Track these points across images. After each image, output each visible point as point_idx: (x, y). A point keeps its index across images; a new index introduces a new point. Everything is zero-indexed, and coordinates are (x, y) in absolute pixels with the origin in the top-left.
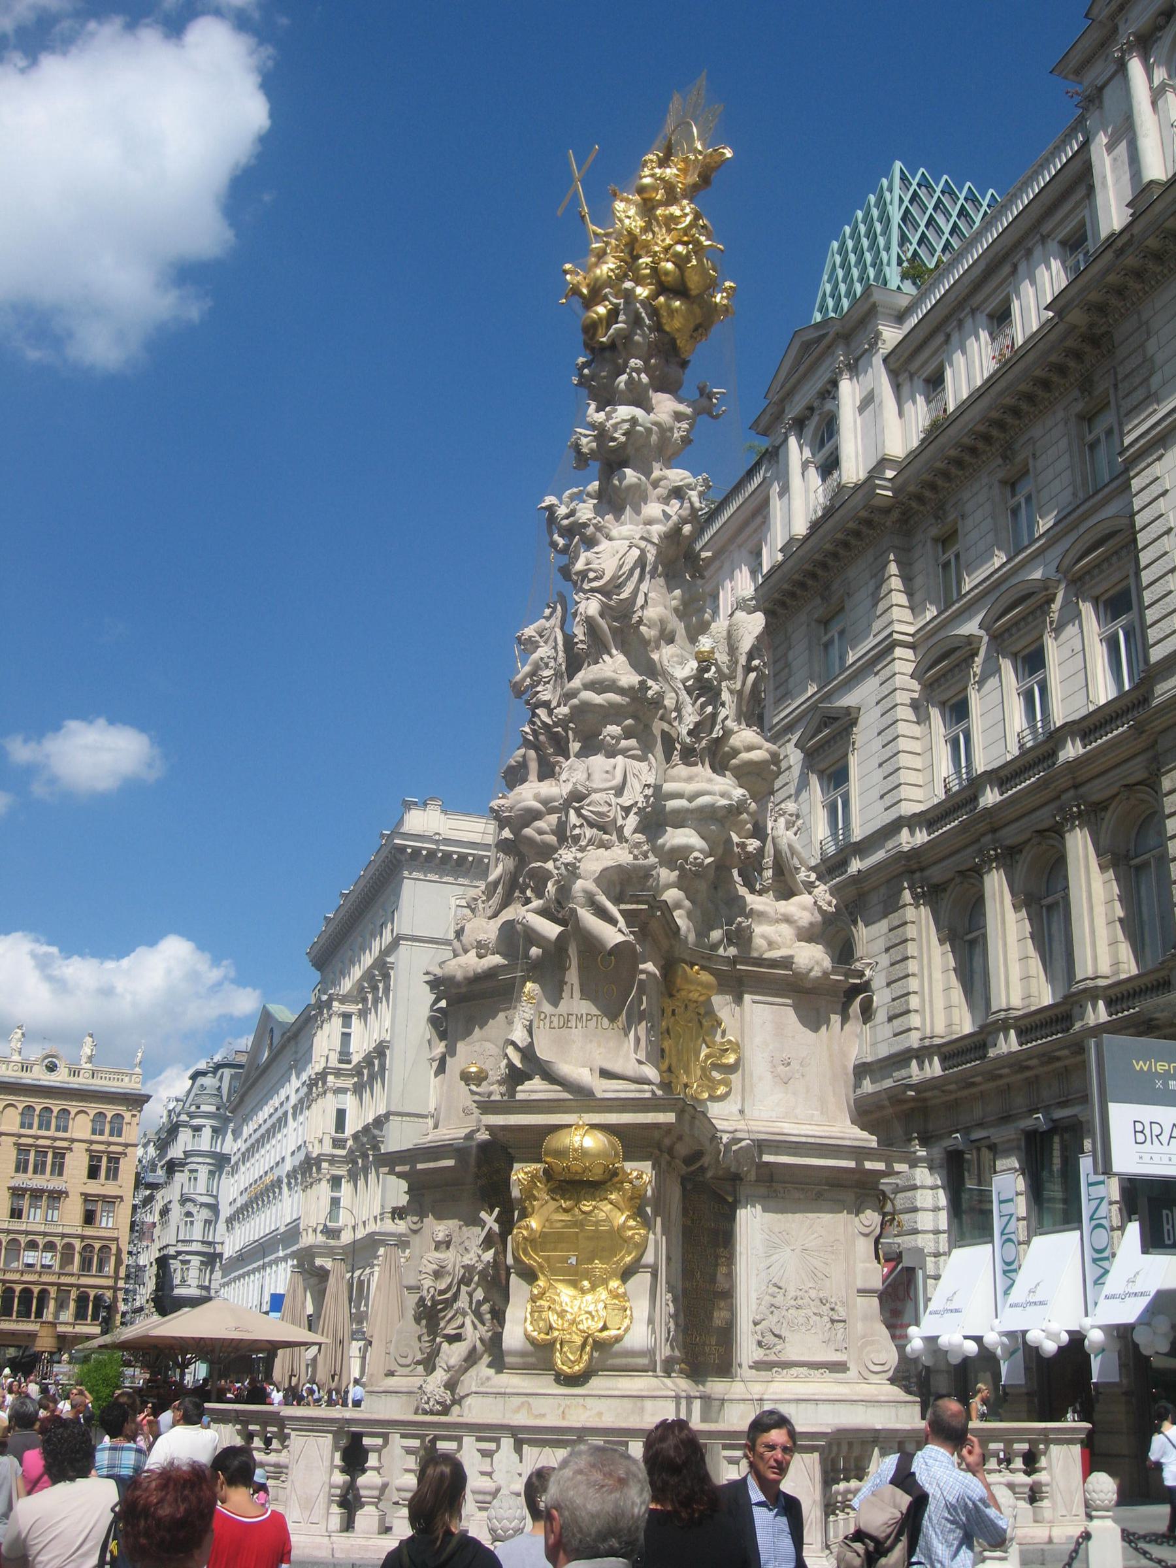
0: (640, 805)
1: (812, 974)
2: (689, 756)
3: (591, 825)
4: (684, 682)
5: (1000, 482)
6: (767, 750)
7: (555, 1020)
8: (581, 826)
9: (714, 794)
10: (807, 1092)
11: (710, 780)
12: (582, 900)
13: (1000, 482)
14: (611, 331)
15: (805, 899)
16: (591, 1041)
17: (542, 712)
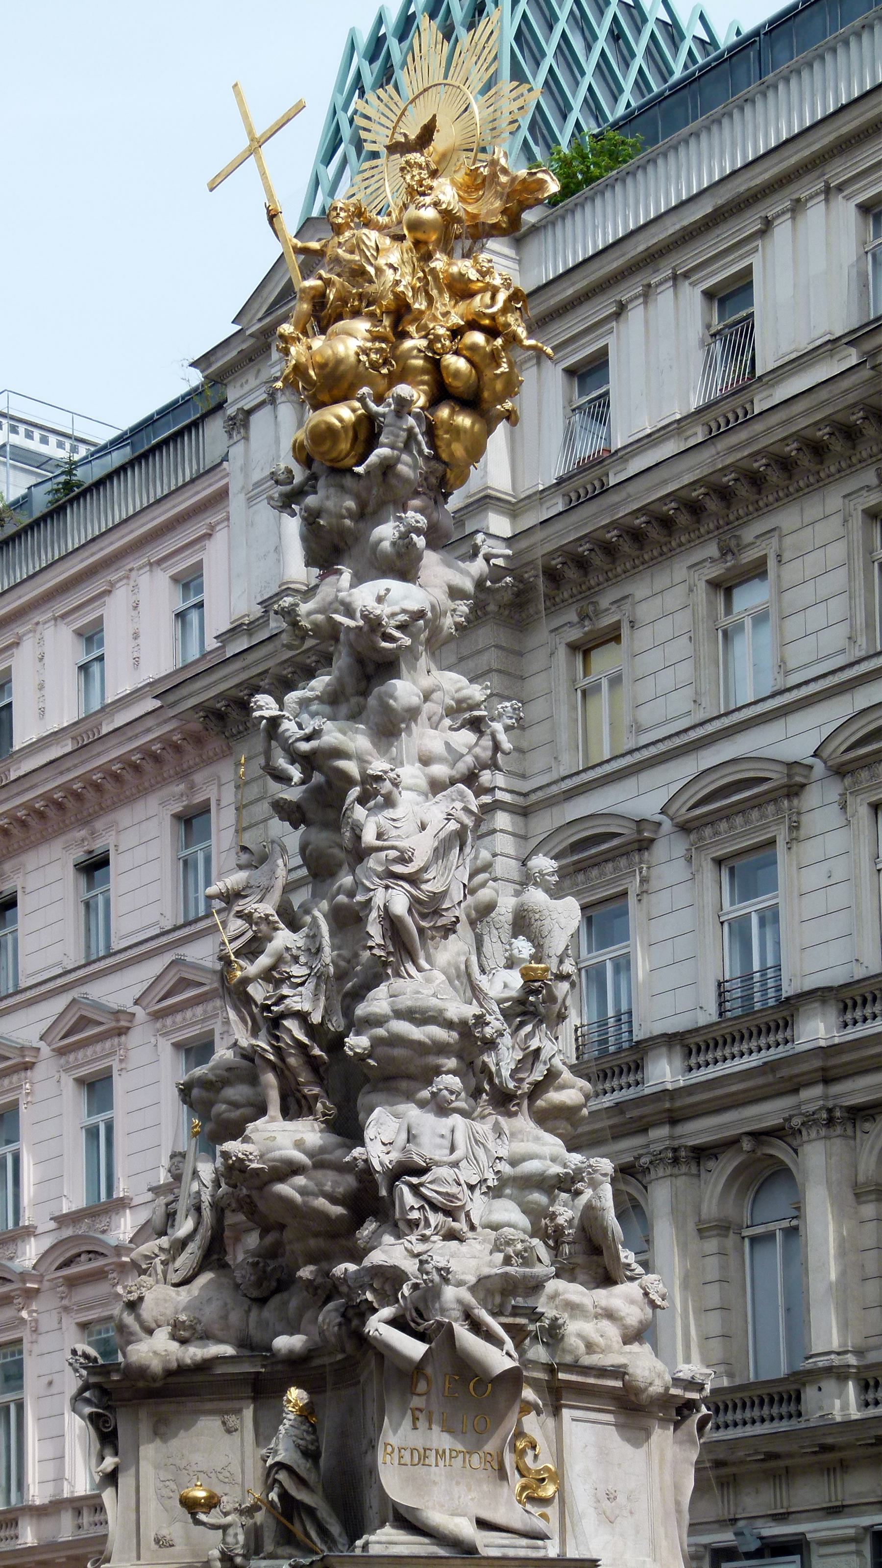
0: (490, 1183)
1: (651, 1389)
2: (504, 1100)
3: (435, 1208)
4: (499, 1002)
5: (709, 582)
6: (581, 1089)
7: (407, 1455)
8: (422, 1208)
9: (544, 1158)
10: (637, 1532)
11: (537, 1139)
12: (457, 1314)
13: (709, 582)
14: (373, 458)
15: (629, 1289)
16: (458, 1483)
17: (290, 1024)
